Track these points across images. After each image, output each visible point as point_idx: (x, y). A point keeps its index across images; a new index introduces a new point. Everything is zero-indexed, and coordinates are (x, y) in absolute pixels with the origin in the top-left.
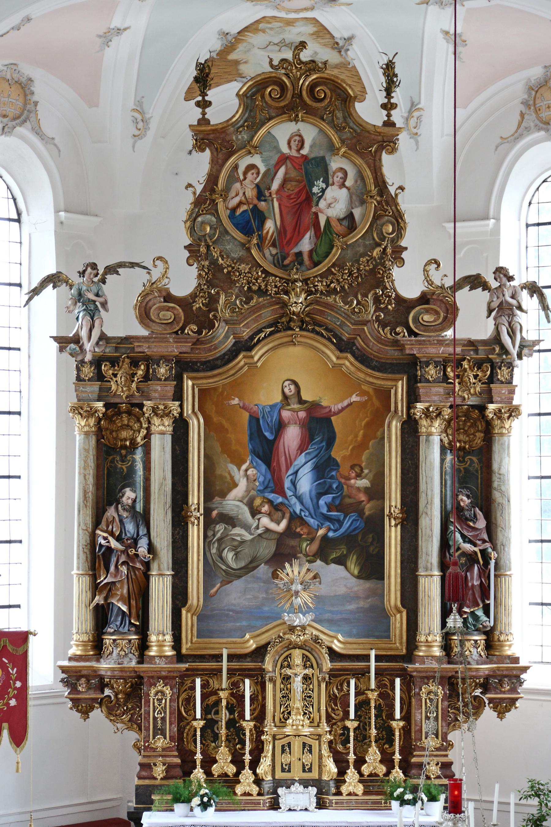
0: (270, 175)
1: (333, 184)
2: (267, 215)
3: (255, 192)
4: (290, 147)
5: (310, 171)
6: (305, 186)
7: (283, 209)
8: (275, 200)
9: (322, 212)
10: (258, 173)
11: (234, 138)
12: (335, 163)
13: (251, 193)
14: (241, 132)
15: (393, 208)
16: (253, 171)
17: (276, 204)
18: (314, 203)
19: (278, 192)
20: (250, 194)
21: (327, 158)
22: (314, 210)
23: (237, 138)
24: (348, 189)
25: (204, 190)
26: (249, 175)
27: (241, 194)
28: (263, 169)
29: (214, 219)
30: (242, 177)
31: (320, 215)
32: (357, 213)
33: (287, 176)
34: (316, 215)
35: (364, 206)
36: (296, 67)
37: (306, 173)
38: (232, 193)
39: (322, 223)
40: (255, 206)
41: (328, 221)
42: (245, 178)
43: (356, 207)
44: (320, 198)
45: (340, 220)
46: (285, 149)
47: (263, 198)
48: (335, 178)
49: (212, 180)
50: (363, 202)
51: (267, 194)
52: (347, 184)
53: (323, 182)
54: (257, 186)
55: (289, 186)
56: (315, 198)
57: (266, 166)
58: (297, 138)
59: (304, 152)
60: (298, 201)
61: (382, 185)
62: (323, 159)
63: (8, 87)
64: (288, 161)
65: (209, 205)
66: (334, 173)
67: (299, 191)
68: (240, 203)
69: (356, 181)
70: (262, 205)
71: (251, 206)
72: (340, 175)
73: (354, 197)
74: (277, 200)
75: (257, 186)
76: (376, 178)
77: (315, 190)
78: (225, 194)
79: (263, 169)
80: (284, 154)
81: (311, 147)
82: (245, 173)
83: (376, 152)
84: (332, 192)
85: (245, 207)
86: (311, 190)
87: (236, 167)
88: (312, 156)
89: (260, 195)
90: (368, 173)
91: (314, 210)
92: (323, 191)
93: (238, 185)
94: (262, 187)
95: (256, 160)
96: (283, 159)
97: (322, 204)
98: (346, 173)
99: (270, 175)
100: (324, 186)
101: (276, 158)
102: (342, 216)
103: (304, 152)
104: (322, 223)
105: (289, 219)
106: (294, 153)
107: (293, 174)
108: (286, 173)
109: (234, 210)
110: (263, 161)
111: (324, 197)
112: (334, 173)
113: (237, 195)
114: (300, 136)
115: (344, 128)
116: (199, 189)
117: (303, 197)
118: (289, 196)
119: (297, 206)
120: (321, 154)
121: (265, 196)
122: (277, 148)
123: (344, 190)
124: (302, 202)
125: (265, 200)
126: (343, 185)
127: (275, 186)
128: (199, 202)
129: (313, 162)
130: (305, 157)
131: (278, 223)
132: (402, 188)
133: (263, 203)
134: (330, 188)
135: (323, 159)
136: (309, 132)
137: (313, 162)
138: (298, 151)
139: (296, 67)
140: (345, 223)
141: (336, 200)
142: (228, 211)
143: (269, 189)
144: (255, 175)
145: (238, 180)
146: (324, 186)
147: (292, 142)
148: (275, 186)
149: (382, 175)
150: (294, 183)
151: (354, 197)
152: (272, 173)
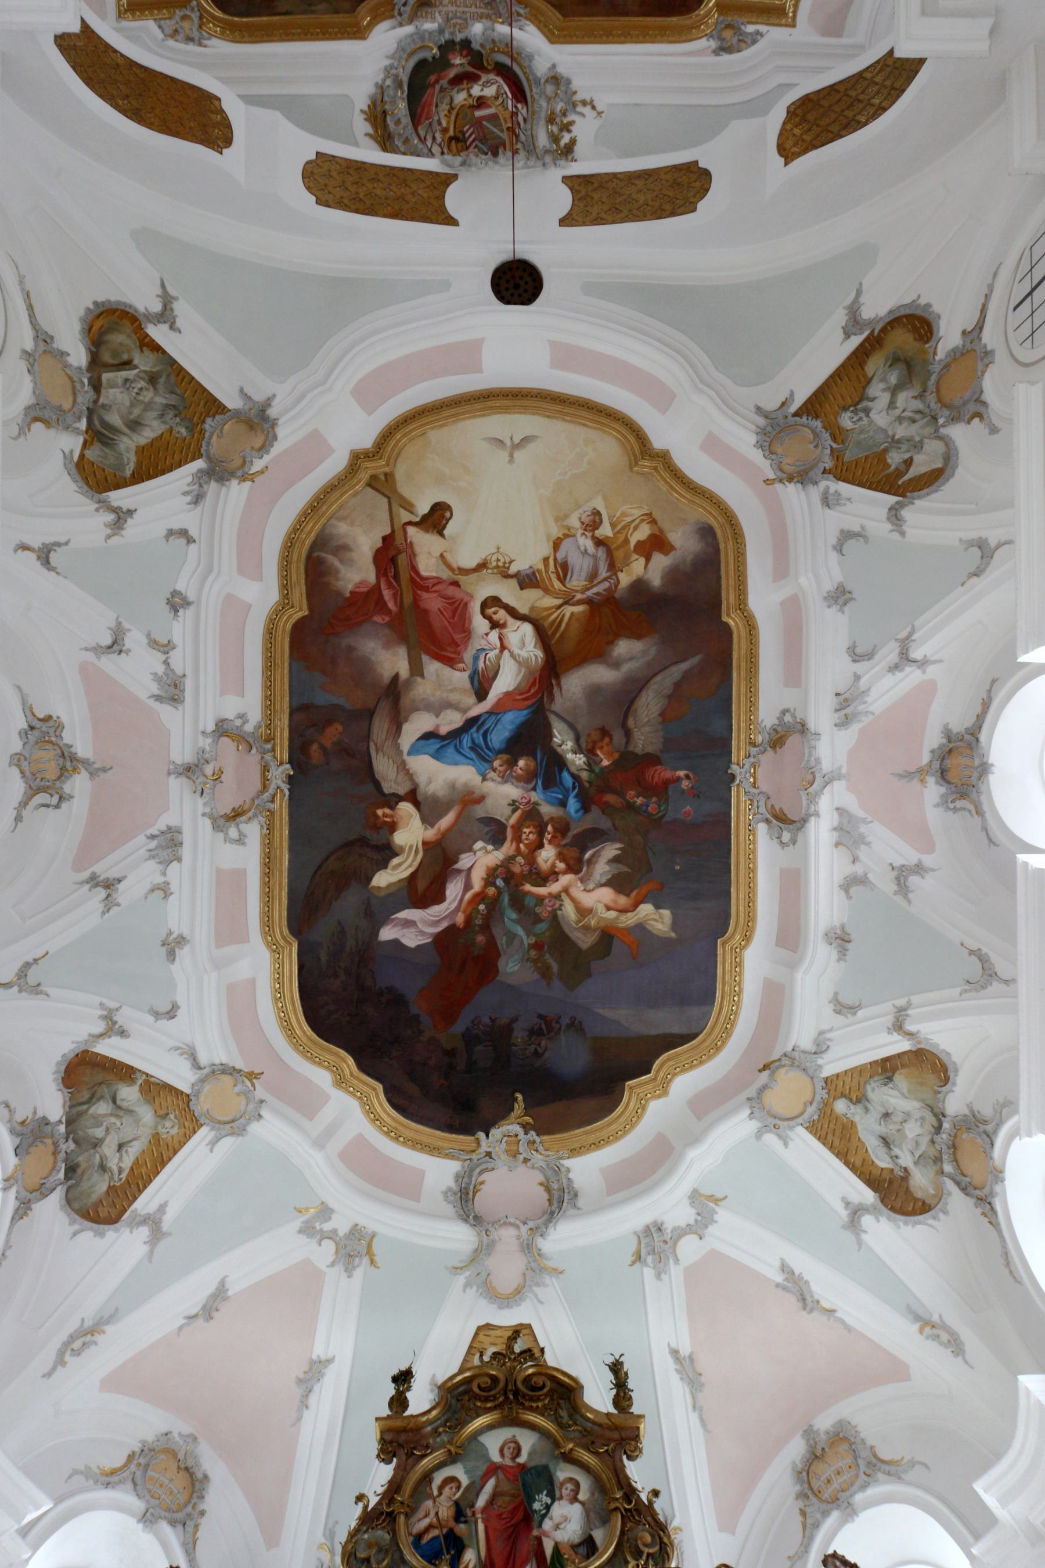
0: (475, 1489)
1: (561, 1498)
2: (466, 1542)
3: (452, 1512)
4: (502, 1455)
5: (529, 1484)
6: (522, 1502)
7: (490, 1533)
8: (480, 1521)
9: (547, 1536)
10: (458, 1488)
11: (431, 1441)
12: (563, 1473)
13: (446, 1512)
14: (440, 1434)
15: (649, 1518)
16: (452, 1485)
17: (481, 1527)
18: (535, 1524)
19: (484, 1510)
20: (445, 1514)
21: (552, 1467)
22: (535, 1533)
23: (434, 1441)
24: (582, 1503)
25: (379, 1503)
26: (447, 1491)
27: (432, 1514)
28: (465, 1481)
29: (387, 1537)
30: (436, 1493)
31: (545, 1540)
32: (598, 1535)
33: (499, 1489)
34: (539, 1541)
35: (607, 1526)
36: (510, 1359)
37: (524, 1485)
38: (421, 1513)
39: (548, 1550)
40: (451, 1531)
41: (557, 1548)
42: (440, 1494)
43: (597, 1528)
44: (544, 1516)
45: (574, 1547)
46: (496, 1458)
47: (463, 1519)
48: (563, 1490)
49: (394, 1487)
50: (605, 1521)
51: (469, 1513)
52: (581, 1497)
53: (547, 1495)
54: (457, 1503)
55: (499, 1502)
56: (536, 1517)
57: (469, 1478)
58: (512, 1445)
59: (522, 1459)
60: (513, 1522)
61: (630, 1492)
62: (546, 1468)
63: (175, 1471)
64: (500, 1473)
65: (384, 1521)
66: (562, 1484)
67: (514, 1509)
68: (430, 1527)
69: (593, 1494)
70: (461, 1529)
71: (445, 1531)
72: (570, 1486)
73: (592, 1515)
74: (483, 1521)
75: (457, 1503)
76: (619, 1482)
77: (536, 1506)
78: (410, 1512)
79: (465, 1481)
80: (493, 1464)
81: (530, 1454)
82: (441, 1488)
83: (613, 1451)
84: (559, 1509)
85: (435, 1532)
86: (531, 1507)
87: (427, 1477)
88: (533, 1464)
89: (460, 1514)
90: (606, 1475)
91: (535, 1533)
92: (548, 1507)
93: (429, 1503)
94: (462, 1504)
95: (457, 1471)
96: (493, 1469)
97: (547, 1525)
98: (577, 1485)
99: (475, 1489)
100: (549, 1501)
101: (484, 1468)
102: (577, 1541)
103: (522, 1459)
104: (548, 1550)
105: (499, 1546)
106: (508, 1462)
107: (506, 1487)
108: (496, 1486)
109: (419, 1536)
110: (466, 1472)
111: (549, 1515)
112: (562, 1484)
113: (426, 1516)
114: (516, 1442)
115: (570, 1426)
116: (373, 1501)
117: (520, 1515)
118: (499, 1516)
119: (511, 1529)
120: (544, 1461)
121: (465, 1516)
122: (486, 1456)
123: (577, 1507)
124: (518, 1520)
125: (466, 1522)
126: (574, 1499)
127: (481, 1502)
128: (368, 1519)
129: (533, 1472)
130: (522, 1466)
131: (483, 1554)
132: (656, 1493)
133: (462, 1526)
134: (556, 1503)
135: (546, 1468)
136: (527, 1440)
137: (533, 1472)
138: (513, 1459)
139: (510, 1359)
140: (583, 1550)
141: (566, 1519)
142: (411, 1539)
143: (472, 1506)
144: (454, 1490)
145: (430, 1495)
146: (549, 1501)
147: (506, 1449)
148: (481, 1502)
149: (628, 1478)
150: (507, 1499)
151: (592, 1515)
152: (478, 1487)
